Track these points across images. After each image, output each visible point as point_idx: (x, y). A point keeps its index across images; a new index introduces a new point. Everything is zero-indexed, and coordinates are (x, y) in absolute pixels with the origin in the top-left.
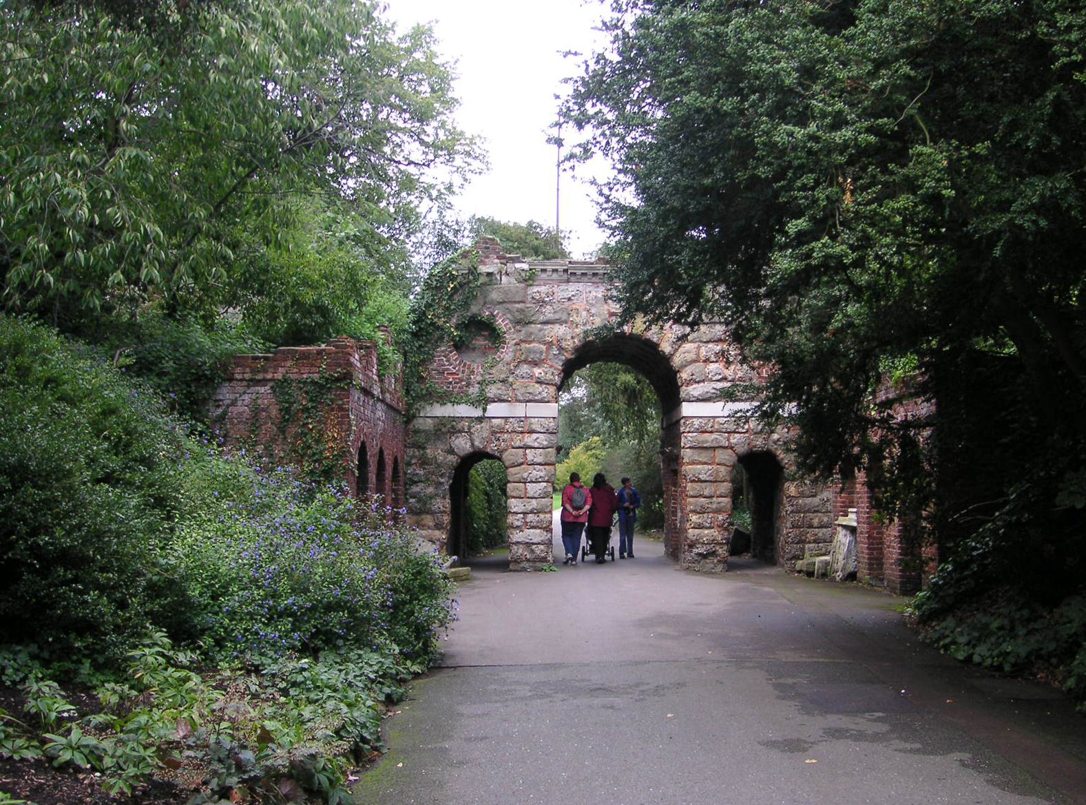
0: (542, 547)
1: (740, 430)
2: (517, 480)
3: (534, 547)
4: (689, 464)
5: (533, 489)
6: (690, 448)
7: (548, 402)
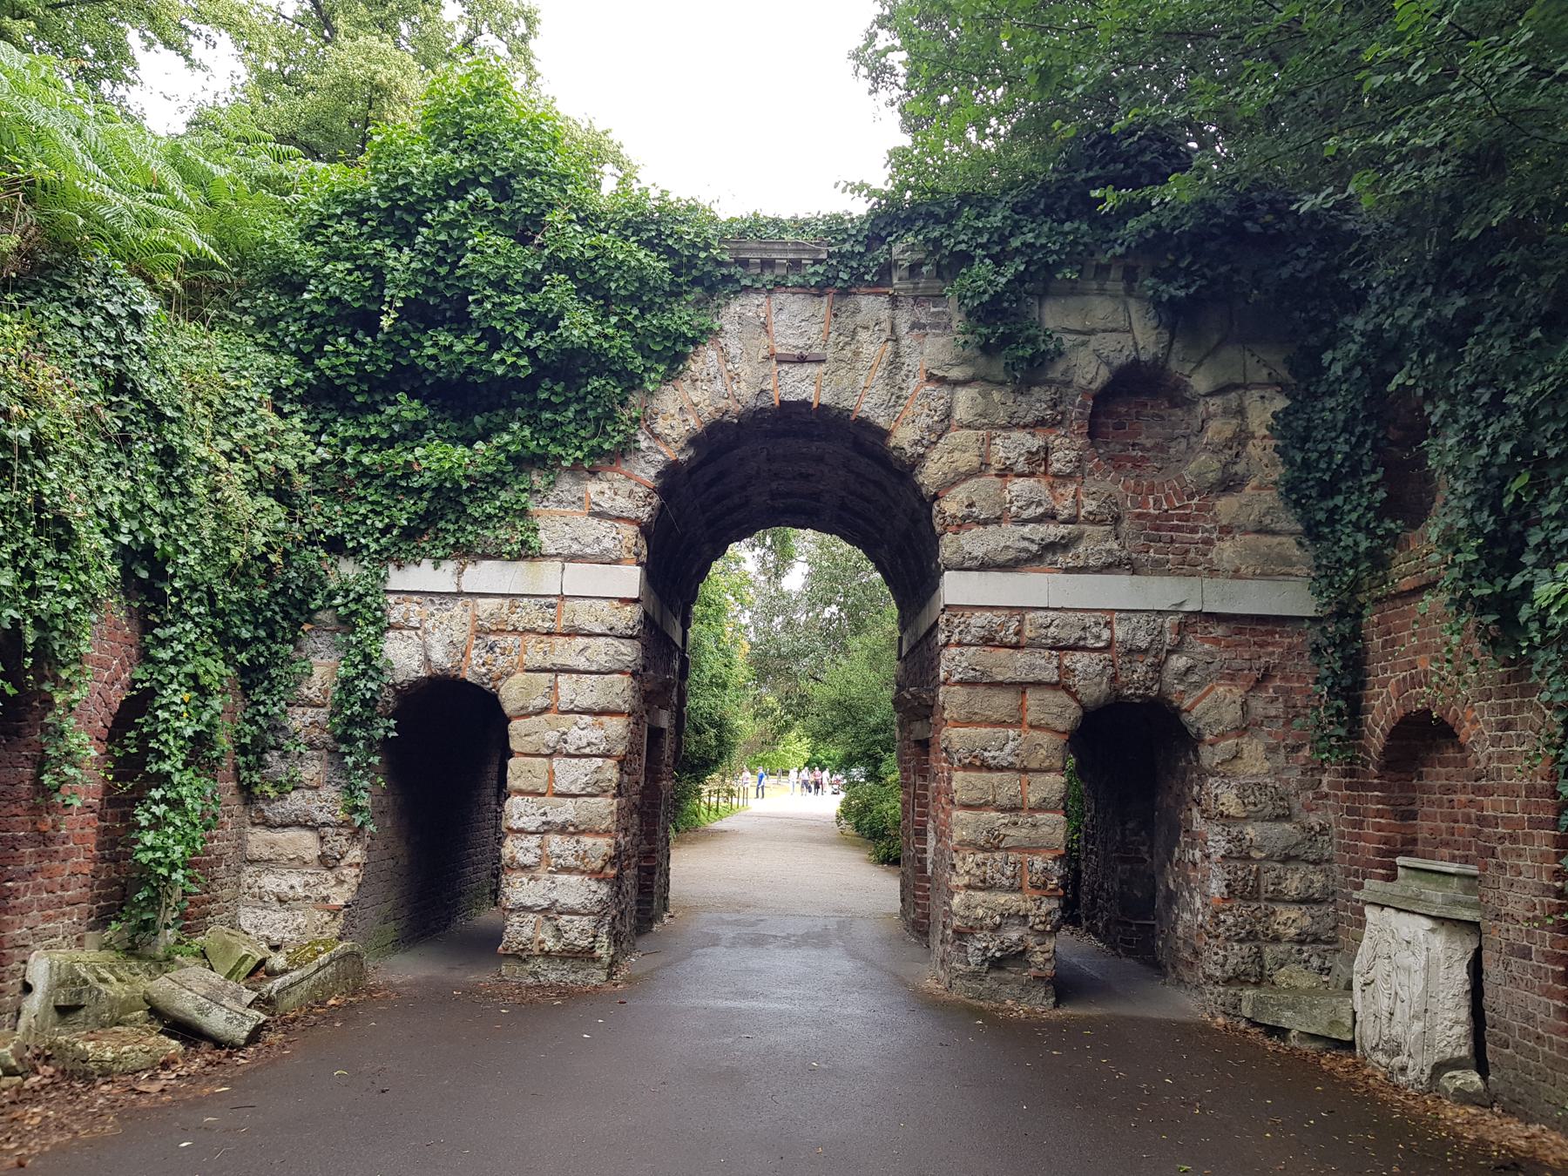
0: (585, 923)
1: (1090, 642)
2: (527, 749)
4: (958, 723)
5: (571, 774)
6: (961, 682)
7: (617, 561)
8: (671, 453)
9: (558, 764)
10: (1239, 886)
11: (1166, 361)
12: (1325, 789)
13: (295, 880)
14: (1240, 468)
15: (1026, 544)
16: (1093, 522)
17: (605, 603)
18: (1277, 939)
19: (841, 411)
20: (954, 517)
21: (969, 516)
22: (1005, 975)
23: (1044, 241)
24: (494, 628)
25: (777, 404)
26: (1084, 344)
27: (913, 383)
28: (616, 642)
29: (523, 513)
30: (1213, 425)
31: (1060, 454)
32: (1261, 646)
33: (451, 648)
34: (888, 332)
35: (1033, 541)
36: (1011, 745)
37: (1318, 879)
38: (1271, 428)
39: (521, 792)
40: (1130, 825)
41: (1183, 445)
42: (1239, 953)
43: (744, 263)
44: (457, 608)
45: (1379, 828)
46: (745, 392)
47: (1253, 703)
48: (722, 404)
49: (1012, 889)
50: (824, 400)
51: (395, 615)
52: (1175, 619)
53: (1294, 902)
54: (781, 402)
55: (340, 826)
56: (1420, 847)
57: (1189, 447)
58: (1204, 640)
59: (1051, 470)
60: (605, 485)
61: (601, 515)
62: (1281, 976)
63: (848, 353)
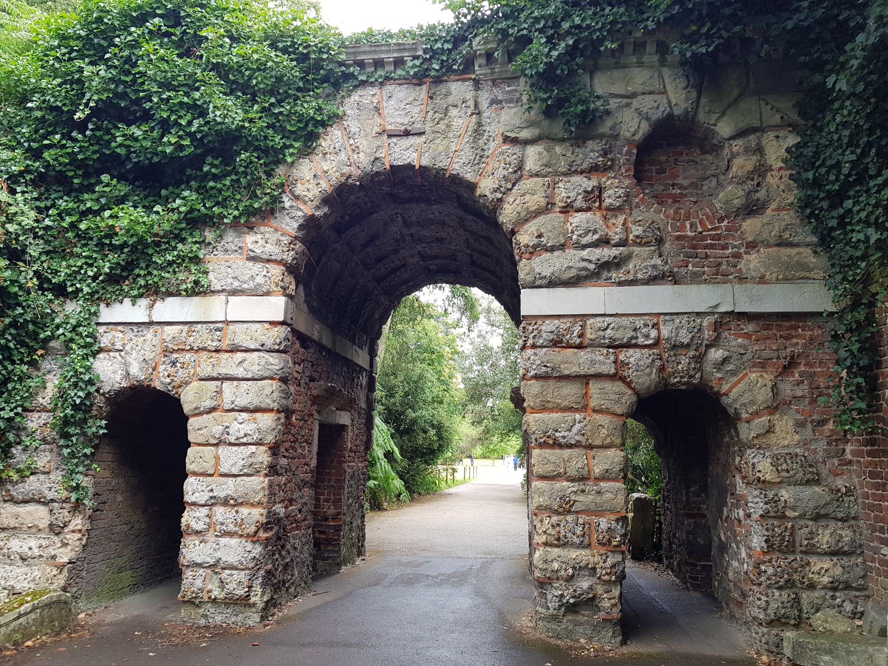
0: (242, 576)
1: (641, 341)
2: (199, 441)
4: (534, 410)
6: (536, 377)
7: (268, 293)
8: (308, 210)
9: (223, 451)
10: (777, 541)
11: (695, 113)
12: (849, 456)
13: (33, 543)
14: (761, 195)
15: (585, 264)
16: (640, 244)
17: (258, 325)
18: (812, 586)
20: (527, 246)
21: (538, 245)
22: (580, 618)
23: (588, 22)
24: (176, 348)
25: (388, 167)
26: (628, 105)
27: (492, 145)
28: (266, 355)
29: (196, 260)
30: (737, 162)
31: (611, 192)
32: (786, 339)
33: (144, 364)
34: (472, 108)
35: (590, 262)
36: (577, 427)
37: (847, 535)
38: (785, 161)
39: (195, 474)
40: (692, 489)
41: (714, 183)
42: (779, 599)
43: (361, 64)
44: (149, 334)
46: (363, 160)
47: (782, 386)
48: (346, 170)
49: (581, 546)
50: (425, 162)
51: (105, 341)
52: (712, 319)
53: (826, 554)
54: (392, 166)
55: (64, 501)
57: (719, 184)
58: (738, 336)
59: (604, 205)
60: (259, 236)
61: (254, 259)
62: (818, 620)
63: (442, 126)
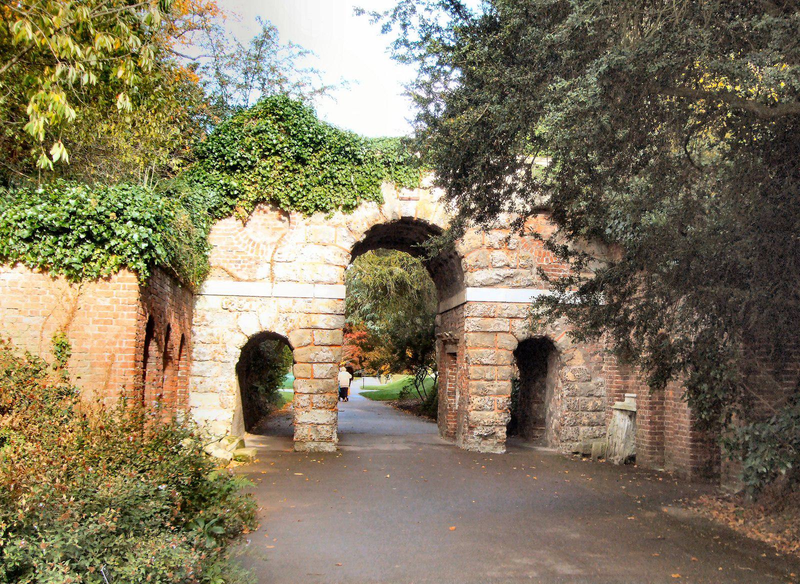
0: (328, 428)
3: (319, 427)
4: (471, 348)
12: (603, 369)
19: (425, 221)
22: (488, 442)
28: (337, 317)
36: (491, 356)
45: (617, 383)
50: (419, 216)
56: (630, 389)
